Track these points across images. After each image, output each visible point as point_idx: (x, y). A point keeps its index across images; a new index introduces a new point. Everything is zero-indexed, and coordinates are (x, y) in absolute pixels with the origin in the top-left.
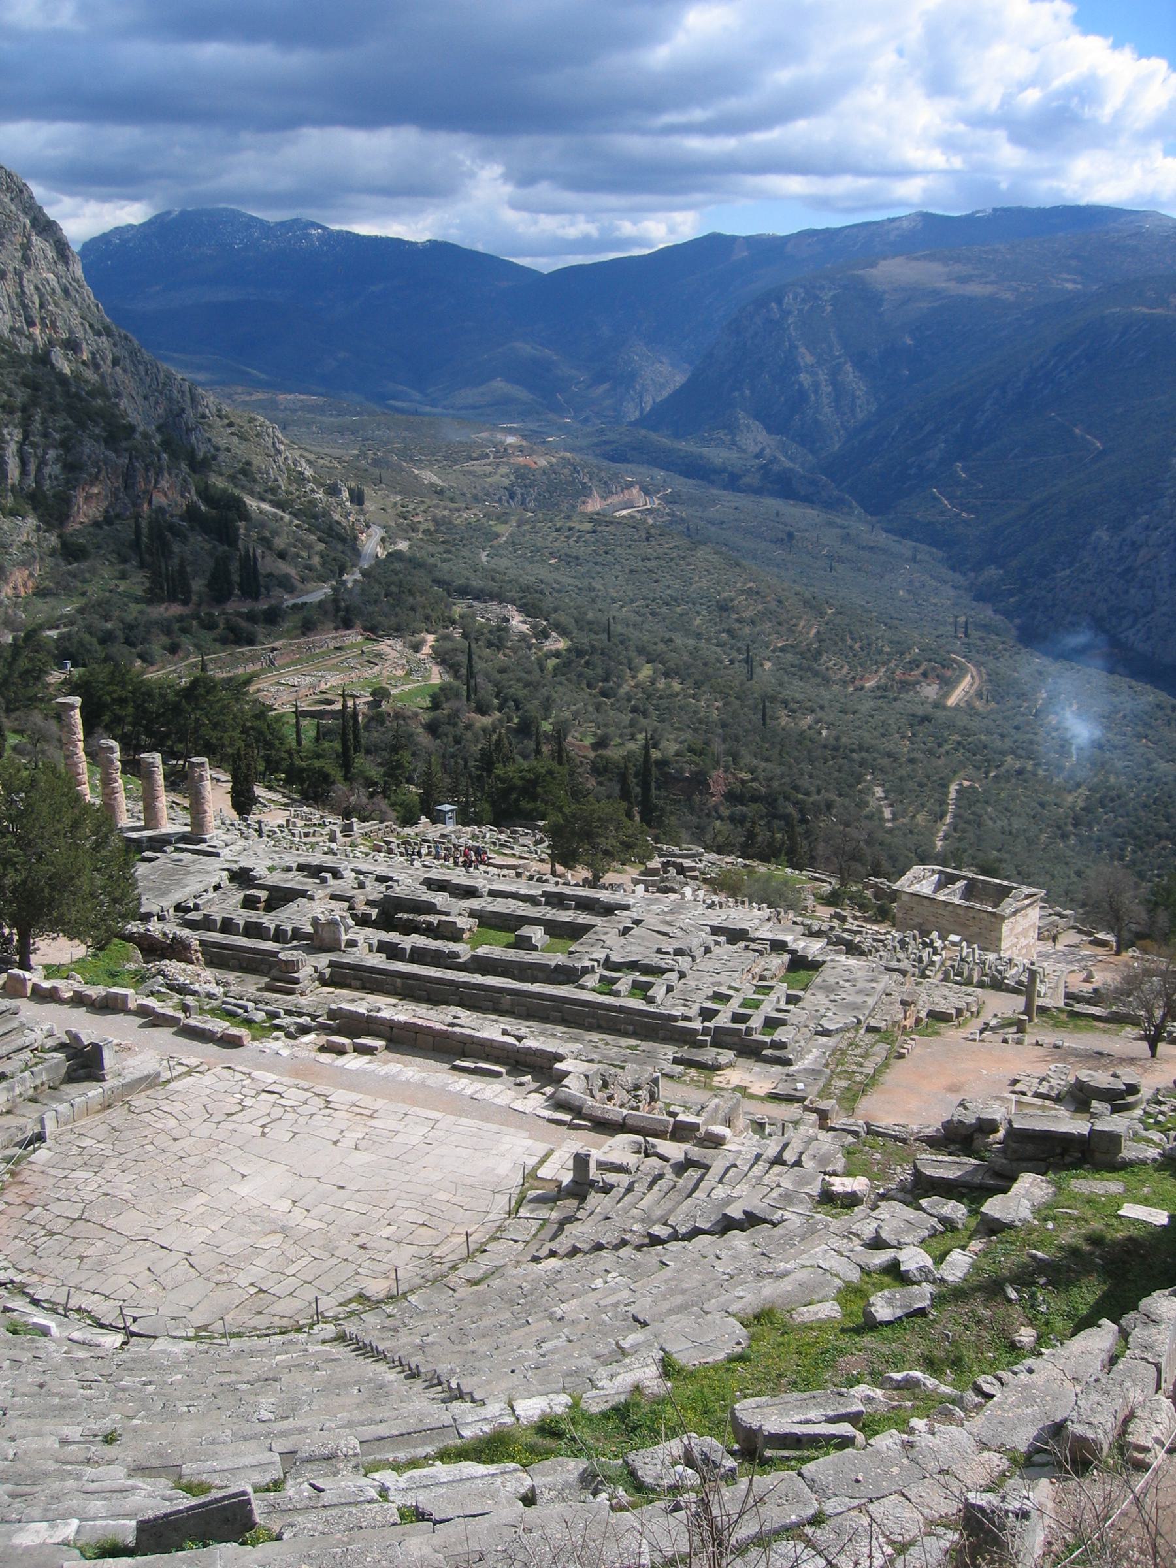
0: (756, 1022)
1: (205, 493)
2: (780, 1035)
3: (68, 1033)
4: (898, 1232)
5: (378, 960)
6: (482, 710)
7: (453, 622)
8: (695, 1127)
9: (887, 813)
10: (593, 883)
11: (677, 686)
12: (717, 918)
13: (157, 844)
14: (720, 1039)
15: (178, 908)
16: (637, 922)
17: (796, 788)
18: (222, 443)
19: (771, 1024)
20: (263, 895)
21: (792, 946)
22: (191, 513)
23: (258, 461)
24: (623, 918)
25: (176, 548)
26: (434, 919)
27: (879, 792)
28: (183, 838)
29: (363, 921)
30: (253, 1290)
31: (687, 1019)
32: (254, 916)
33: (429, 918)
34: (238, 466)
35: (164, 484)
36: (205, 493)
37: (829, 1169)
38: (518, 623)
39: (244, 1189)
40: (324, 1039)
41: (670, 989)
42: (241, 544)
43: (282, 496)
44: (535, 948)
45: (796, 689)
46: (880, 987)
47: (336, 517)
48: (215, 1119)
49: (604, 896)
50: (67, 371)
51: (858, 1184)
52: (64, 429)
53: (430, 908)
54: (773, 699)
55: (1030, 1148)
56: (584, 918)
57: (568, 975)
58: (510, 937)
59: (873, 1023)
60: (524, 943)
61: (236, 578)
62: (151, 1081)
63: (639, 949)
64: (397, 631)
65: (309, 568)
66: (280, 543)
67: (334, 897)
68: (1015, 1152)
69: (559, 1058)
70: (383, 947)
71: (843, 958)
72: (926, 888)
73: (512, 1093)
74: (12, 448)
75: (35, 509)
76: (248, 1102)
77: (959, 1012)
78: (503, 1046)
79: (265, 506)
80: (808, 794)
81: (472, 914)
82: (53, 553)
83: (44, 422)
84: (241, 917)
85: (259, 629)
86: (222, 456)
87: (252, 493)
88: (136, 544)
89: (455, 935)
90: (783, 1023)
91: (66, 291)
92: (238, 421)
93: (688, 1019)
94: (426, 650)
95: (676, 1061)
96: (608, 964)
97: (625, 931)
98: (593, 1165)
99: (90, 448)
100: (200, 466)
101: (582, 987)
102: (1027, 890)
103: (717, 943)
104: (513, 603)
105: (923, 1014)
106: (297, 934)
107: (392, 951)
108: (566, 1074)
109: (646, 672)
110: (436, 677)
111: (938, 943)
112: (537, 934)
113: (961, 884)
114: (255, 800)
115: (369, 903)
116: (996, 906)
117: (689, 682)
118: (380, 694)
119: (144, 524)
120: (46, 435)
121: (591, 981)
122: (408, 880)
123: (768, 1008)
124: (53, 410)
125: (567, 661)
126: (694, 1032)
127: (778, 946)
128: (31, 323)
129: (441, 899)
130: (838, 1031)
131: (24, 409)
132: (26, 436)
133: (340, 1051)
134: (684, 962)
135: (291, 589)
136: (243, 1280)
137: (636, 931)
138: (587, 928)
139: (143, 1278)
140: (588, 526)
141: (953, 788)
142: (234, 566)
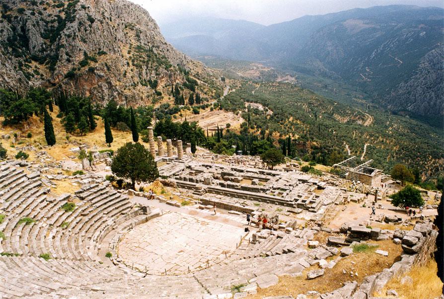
0: (307, 202)
1: (188, 80)
2: (314, 205)
3: (139, 204)
4: (320, 255)
5: (219, 187)
6: (252, 128)
7: (245, 108)
8: (284, 228)
9: (349, 151)
10: (271, 169)
11: (299, 122)
12: (301, 177)
13: (171, 160)
14: (299, 206)
15: (174, 175)
16: (280, 178)
18: (192, 68)
19: (311, 202)
20: (194, 172)
21: (318, 184)
22: (185, 84)
23: (200, 72)
24: (277, 177)
25: (181, 92)
26: (233, 178)
27: (347, 146)
28: (176, 159)
29: (217, 178)
30: (175, 265)
31: (291, 201)
32: (191, 177)
34: (196, 73)
36: (188, 80)
37: (310, 239)
38: (261, 108)
39: (176, 240)
41: (287, 194)
42: (196, 91)
44: (256, 184)
46: (338, 194)
47: (218, 84)
48: (171, 224)
49: (273, 172)
50: (156, 53)
51: (316, 243)
52: (157, 66)
53: (232, 175)
57: (264, 191)
58: (250, 182)
59: (336, 202)
60: (253, 183)
61: (194, 98)
62: (157, 215)
63: (280, 184)
64: (234, 111)
65: (212, 96)
67: (209, 172)
68: (352, 236)
69: (253, 211)
71: (330, 187)
73: (241, 219)
74: (144, 71)
75: (149, 84)
77: (358, 200)
78: (240, 208)
79: (202, 82)
81: (242, 176)
82: (154, 93)
83: (151, 64)
84: (188, 177)
85: (201, 110)
86: (192, 71)
87: (199, 79)
89: (238, 181)
90: (314, 202)
91: (156, 35)
92: (195, 63)
93: (291, 201)
95: (288, 211)
98: (257, 237)
99: (162, 70)
100: (187, 73)
101: (266, 194)
102: (378, 170)
103: (299, 183)
104: (259, 103)
105: (349, 200)
106: (201, 181)
107: (222, 185)
108: (254, 215)
109: (291, 119)
110: (242, 121)
111: (355, 183)
112: (256, 181)
114: (196, 150)
115: (218, 174)
116: (370, 174)
118: (228, 126)
119: (174, 87)
120: (152, 67)
121: (268, 192)
122: (227, 168)
123: (310, 199)
124: (153, 62)
125: (272, 118)
126: (293, 205)
128: (148, 42)
129: (234, 172)
130: (327, 205)
131: (147, 62)
132: (147, 68)
134: (291, 187)
135: (208, 101)
137: (280, 180)
138: (269, 179)
139: (151, 261)
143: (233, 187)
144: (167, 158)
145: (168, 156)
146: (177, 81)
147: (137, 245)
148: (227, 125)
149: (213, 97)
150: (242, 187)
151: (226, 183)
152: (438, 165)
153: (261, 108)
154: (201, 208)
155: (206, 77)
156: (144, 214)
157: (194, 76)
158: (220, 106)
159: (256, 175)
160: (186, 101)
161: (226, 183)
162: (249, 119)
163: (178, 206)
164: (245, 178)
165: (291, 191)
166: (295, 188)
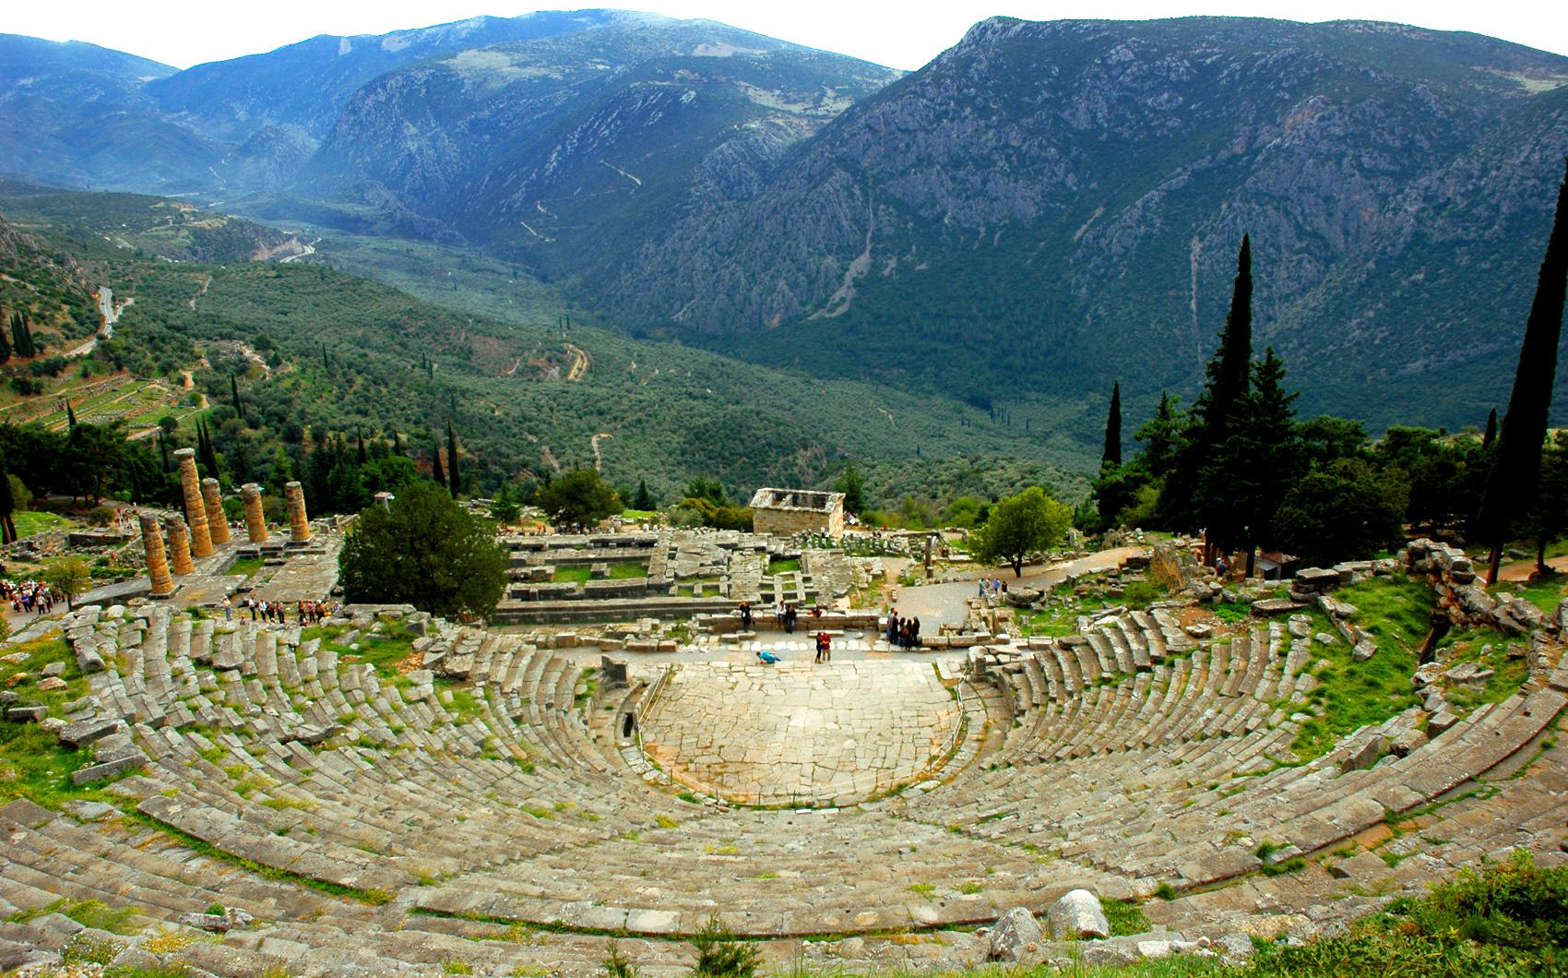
5: (518, 603)
6: (254, 425)
9: (556, 465)
11: (384, 391)
17: (500, 455)
28: (288, 545)
33: (524, 570)
40: (714, 638)
43: (18, 268)
45: (467, 382)
53: (522, 563)
54: (453, 390)
55: (1311, 586)
56: (639, 553)
58: (587, 572)
61: (10, 340)
62: (666, 681)
63: (683, 566)
65: (66, 326)
66: (35, 308)
69: (874, 619)
70: (515, 594)
72: (767, 503)
76: (732, 680)
78: (835, 619)
80: (508, 457)
81: (548, 562)
85: (45, 379)
89: (546, 578)
94: (190, 383)
96: (683, 579)
104: (242, 338)
107: (526, 596)
109: (359, 380)
113: (789, 497)
117: (393, 385)
121: (673, 590)
136: (863, 764)
140: (273, 273)
141: (594, 439)
143: (559, 594)
144: (253, 547)
145: (252, 540)
147: (715, 759)
148: (162, 423)
149: (70, 333)
150: (588, 590)
151: (534, 588)
152: (796, 470)
154: (727, 641)
155: (16, 257)
156: (619, 686)
158: (112, 358)
162: (235, 394)
163: (671, 649)
165: (729, 577)
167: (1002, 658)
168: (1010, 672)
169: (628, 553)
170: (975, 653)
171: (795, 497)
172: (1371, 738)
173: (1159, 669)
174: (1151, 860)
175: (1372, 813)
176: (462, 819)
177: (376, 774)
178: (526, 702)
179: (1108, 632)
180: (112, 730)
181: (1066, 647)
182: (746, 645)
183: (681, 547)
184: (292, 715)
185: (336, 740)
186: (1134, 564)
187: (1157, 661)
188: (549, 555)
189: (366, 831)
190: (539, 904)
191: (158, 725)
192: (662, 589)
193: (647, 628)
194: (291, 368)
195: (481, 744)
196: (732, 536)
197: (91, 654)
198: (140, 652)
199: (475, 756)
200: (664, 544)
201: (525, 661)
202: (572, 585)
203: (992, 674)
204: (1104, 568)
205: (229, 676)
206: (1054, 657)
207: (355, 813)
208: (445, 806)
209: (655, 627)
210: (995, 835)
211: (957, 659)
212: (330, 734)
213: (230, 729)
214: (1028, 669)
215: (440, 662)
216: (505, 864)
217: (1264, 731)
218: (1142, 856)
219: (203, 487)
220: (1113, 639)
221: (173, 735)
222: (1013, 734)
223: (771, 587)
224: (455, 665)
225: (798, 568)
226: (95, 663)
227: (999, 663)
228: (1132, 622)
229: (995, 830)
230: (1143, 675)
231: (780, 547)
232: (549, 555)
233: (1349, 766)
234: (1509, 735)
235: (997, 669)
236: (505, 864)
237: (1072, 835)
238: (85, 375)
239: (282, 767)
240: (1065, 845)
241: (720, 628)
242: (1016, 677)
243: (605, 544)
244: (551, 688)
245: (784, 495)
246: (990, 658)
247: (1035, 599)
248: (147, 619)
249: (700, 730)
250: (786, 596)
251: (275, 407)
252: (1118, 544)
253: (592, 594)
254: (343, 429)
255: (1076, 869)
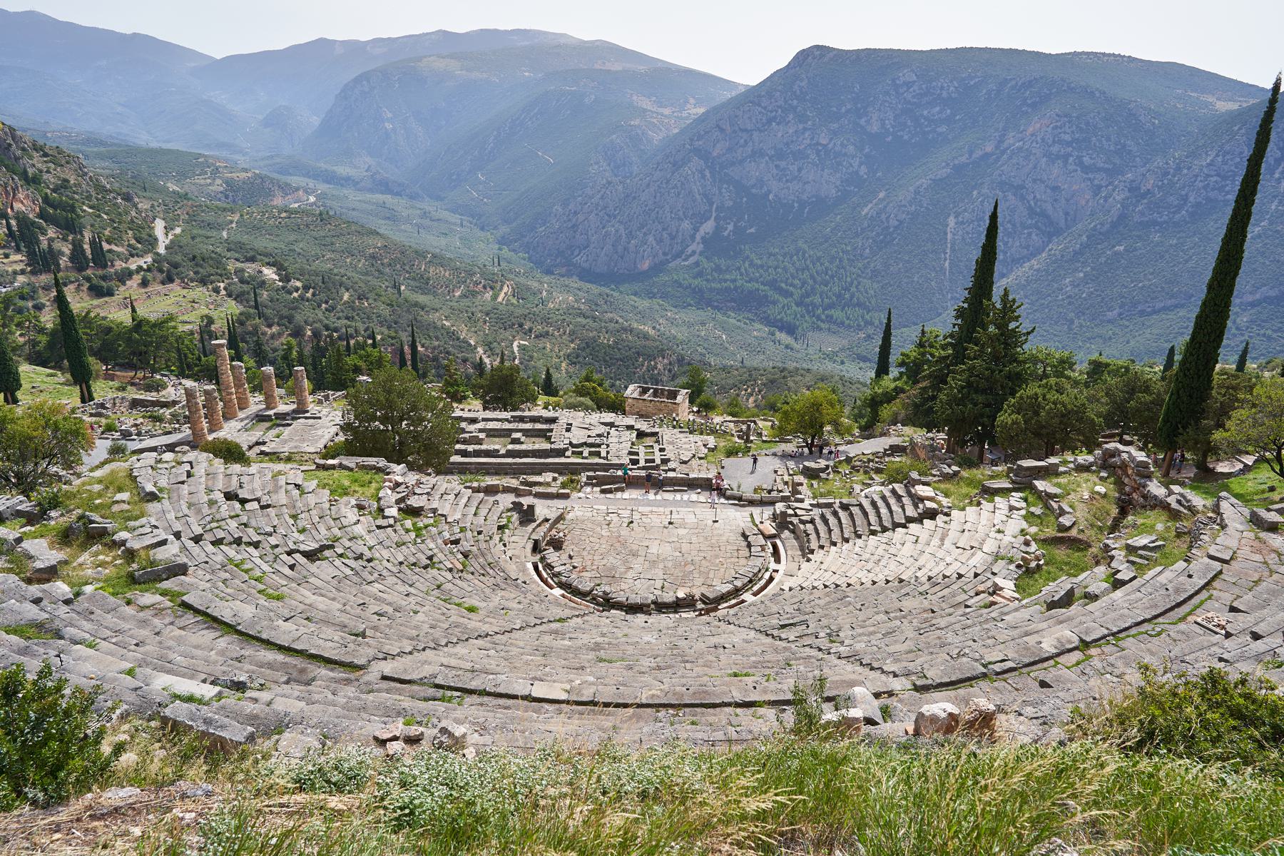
1: (46, 199)
26: (467, 435)
28: (294, 411)
35: (21, 196)
36: (46, 199)
38: (270, 273)
40: (598, 489)
54: (416, 304)
62: (561, 518)
63: (578, 436)
64: (203, 282)
69: (709, 480)
72: (636, 395)
81: (481, 431)
86: (45, 176)
88: (11, 234)
89: (480, 442)
90: (669, 460)
97: (568, 430)
107: (464, 454)
127: (630, 428)
133: (610, 491)
140: (284, 215)
141: (516, 344)
142: (86, 247)
143: (488, 454)
145: (268, 408)
146: (17, 206)
151: (470, 448)
153: (270, 273)
154: (603, 491)
157: (54, 191)
158: (168, 271)
159: (507, 426)
160: (64, 261)
161: (470, 448)
162: (256, 301)
164: (492, 433)
166: (610, 440)
167: (799, 512)
168: (803, 522)
169: (539, 426)
170: (780, 507)
171: (656, 391)
172: (1069, 586)
173: (911, 525)
174: (905, 664)
175: (1070, 642)
176: (416, 612)
177: (355, 579)
178: (463, 530)
179: (877, 498)
180: (164, 542)
181: (845, 507)
182: (619, 495)
183: (577, 425)
184: (296, 535)
185: (327, 553)
186: (894, 450)
187: (910, 520)
188: (480, 425)
189: (344, 618)
190: (469, 675)
191: (197, 539)
192: (560, 453)
193: (549, 479)
194: (299, 284)
195: (430, 558)
196: (609, 417)
197: (149, 488)
198: (185, 486)
199: (425, 567)
200: (563, 421)
201: (464, 500)
202: (497, 447)
203: (791, 523)
204: (874, 450)
205: (248, 506)
206: (835, 514)
207: (340, 606)
208: (404, 603)
209: (555, 479)
210: (792, 638)
211: (768, 512)
212: (323, 548)
213: (249, 544)
214: (818, 521)
215: (401, 500)
216: (446, 645)
217: (989, 575)
218: (896, 661)
219: (232, 368)
220: (880, 503)
221: (210, 548)
222: (805, 565)
223: (637, 454)
224: (414, 502)
225: (657, 442)
226: (152, 494)
227: (796, 515)
228: (894, 492)
229: (791, 634)
230: (900, 530)
231: (643, 426)
232: (480, 425)
233: (1052, 605)
234: (1177, 591)
235: (795, 520)
236: (446, 645)
237: (847, 642)
238: (144, 283)
239: (287, 571)
240: (842, 649)
241: (599, 482)
242: (809, 527)
243: (522, 419)
244: (481, 520)
245: (649, 389)
246: (790, 512)
247: (823, 470)
248: (191, 463)
249: (585, 553)
250: (647, 461)
251: (285, 312)
252: (883, 434)
253: (510, 454)
254: (336, 330)
255: (849, 667)
